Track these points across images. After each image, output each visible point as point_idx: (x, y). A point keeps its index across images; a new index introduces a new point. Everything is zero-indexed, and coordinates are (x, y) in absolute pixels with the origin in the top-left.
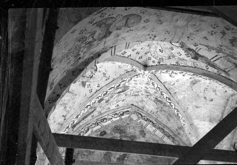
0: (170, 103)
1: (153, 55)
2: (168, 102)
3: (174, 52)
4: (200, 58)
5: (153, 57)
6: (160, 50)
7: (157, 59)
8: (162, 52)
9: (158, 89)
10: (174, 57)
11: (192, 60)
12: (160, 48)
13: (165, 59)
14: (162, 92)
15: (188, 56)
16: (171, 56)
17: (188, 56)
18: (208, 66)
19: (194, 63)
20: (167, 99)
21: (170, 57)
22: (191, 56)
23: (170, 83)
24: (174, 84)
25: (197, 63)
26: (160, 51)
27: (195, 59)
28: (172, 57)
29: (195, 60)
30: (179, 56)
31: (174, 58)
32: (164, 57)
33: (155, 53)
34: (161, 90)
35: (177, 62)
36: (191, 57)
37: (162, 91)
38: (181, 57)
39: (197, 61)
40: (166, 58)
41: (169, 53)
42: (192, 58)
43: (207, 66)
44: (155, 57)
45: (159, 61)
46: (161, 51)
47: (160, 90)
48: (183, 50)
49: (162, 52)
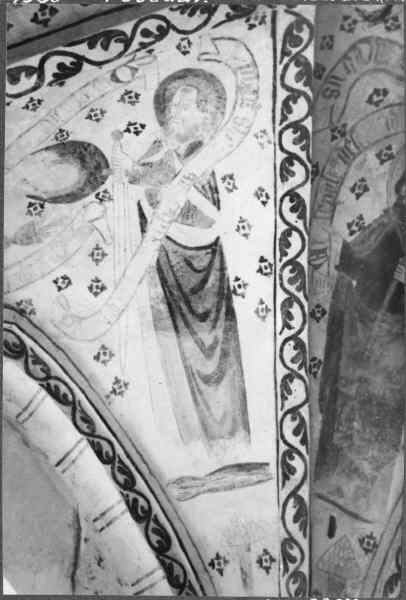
0: (40, 70)
1: (365, 48)
2: (43, 61)
3: (365, 160)
4: (354, 283)
5: (353, 47)
6: (385, 92)
7: (340, 65)
8: (371, 97)
9: (152, 25)
10: (340, 156)
11: (337, 247)
12: (392, 97)
13: (332, 108)
14: (127, 43)
15: (354, 228)
16: (347, 142)
17: (354, 228)
18: (326, 316)
19: (324, 251)
20: (68, 61)
21: (343, 135)
22: (355, 243)
23: (133, 64)
24: (118, 81)
25: (326, 265)
26: (377, 92)
27: (341, 258)
28: (342, 144)
29: (335, 259)
30: (349, 183)
31: (335, 155)
32: (341, 102)
33: (371, 65)
34: (138, 38)
35: (321, 168)
36: (350, 239)
37: (135, 45)
38: (346, 195)
39: (337, 267)
40: (337, 113)
41: (363, 134)
42: (346, 246)
43: (324, 313)
44: (352, 55)
45: (326, 73)
46: (375, 99)
47: (146, 33)
48: (386, 211)
49: (370, 101)
